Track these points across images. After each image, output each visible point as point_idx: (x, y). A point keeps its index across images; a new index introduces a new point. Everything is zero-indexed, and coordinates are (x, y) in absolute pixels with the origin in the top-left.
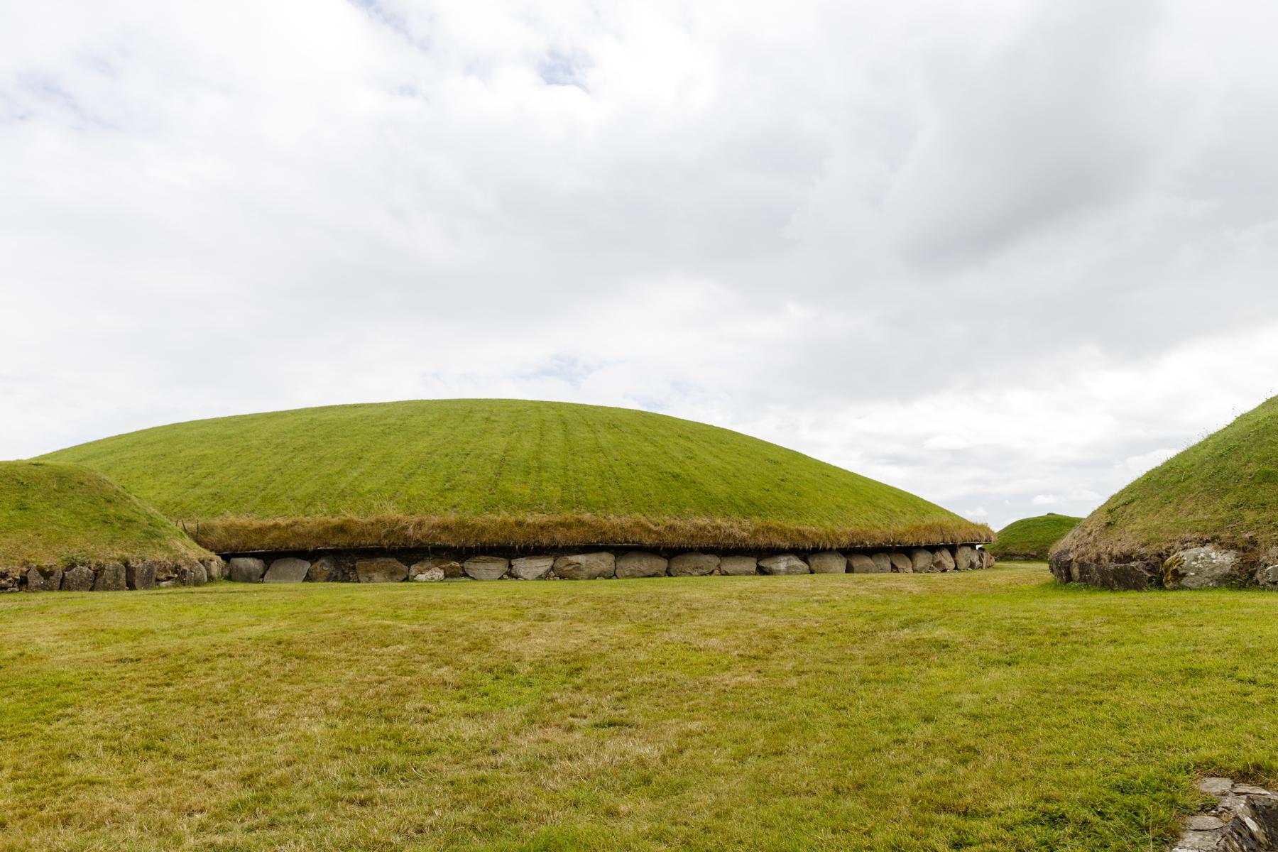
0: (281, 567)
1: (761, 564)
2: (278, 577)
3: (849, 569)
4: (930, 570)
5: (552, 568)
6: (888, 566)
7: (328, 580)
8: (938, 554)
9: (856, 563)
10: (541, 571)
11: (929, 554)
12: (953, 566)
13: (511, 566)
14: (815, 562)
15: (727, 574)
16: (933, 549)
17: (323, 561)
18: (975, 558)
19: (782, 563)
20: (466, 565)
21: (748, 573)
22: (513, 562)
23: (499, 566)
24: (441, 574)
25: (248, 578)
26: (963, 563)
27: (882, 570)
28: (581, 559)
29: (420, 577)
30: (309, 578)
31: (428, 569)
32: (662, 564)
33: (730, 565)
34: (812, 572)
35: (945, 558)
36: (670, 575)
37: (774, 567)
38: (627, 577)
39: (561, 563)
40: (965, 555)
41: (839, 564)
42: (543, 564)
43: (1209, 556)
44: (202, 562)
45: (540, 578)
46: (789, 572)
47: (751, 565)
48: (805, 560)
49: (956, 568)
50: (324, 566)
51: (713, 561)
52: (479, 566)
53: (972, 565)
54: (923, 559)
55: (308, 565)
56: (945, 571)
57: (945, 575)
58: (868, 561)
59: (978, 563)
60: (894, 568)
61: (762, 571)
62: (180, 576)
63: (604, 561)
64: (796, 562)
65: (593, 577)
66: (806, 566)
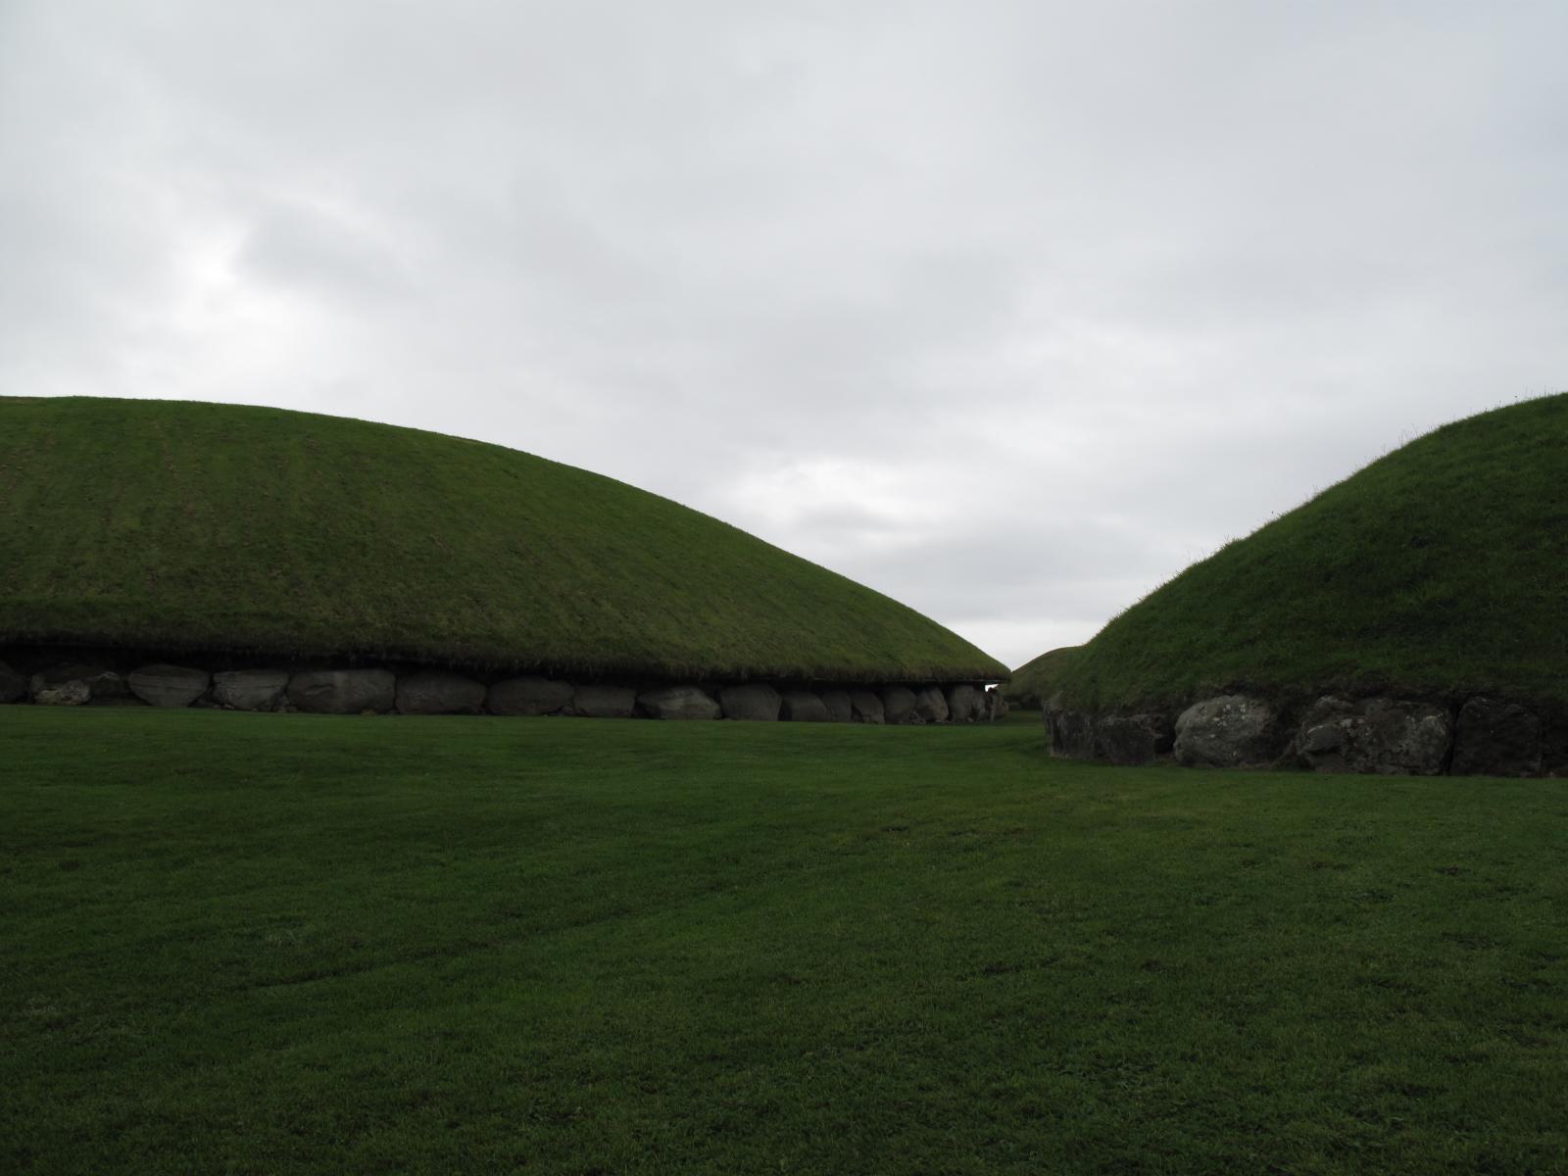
1: (642, 699)
3: (785, 715)
4: (910, 721)
5: (285, 690)
6: (848, 711)
8: (924, 695)
9: (799, 704)
10: (266, 694)
11: (912, 695)
12: (946, 714)
13: (212, 684)
14: (730, 698)
15: (583, 714)
16: (918, 687)
19: (677, 701)
20: (132, 678)
21: (618, 714)
22: (216, 678)
23: (193, 685)
24: (85, 693)
26: (962, 710)
28: (339, 678)
29: (47, 694)
31: (63, 681)
32: (475, 692)
33: (591, 700)
35: (936, 702)
36: (490, 713)
37: (663, 706)
38: (415, 711)
40: (963, 697)
41: (766, 703)
42: (264, 686)
43: (1237, 710)
45: (261, 707)
46: (687, 714)
47: (624, 700)
48: (716, 698)
49: (949, 718)
51: (560, 691)
53: (974, 713)
54: (901, 702)
56: (931, 721)
57: (931, 729)
58: (816, 703)
59: (983, 711)
60: (857, 716)
61: (643, 712)
64: (700, 699)
65: (356, 709)
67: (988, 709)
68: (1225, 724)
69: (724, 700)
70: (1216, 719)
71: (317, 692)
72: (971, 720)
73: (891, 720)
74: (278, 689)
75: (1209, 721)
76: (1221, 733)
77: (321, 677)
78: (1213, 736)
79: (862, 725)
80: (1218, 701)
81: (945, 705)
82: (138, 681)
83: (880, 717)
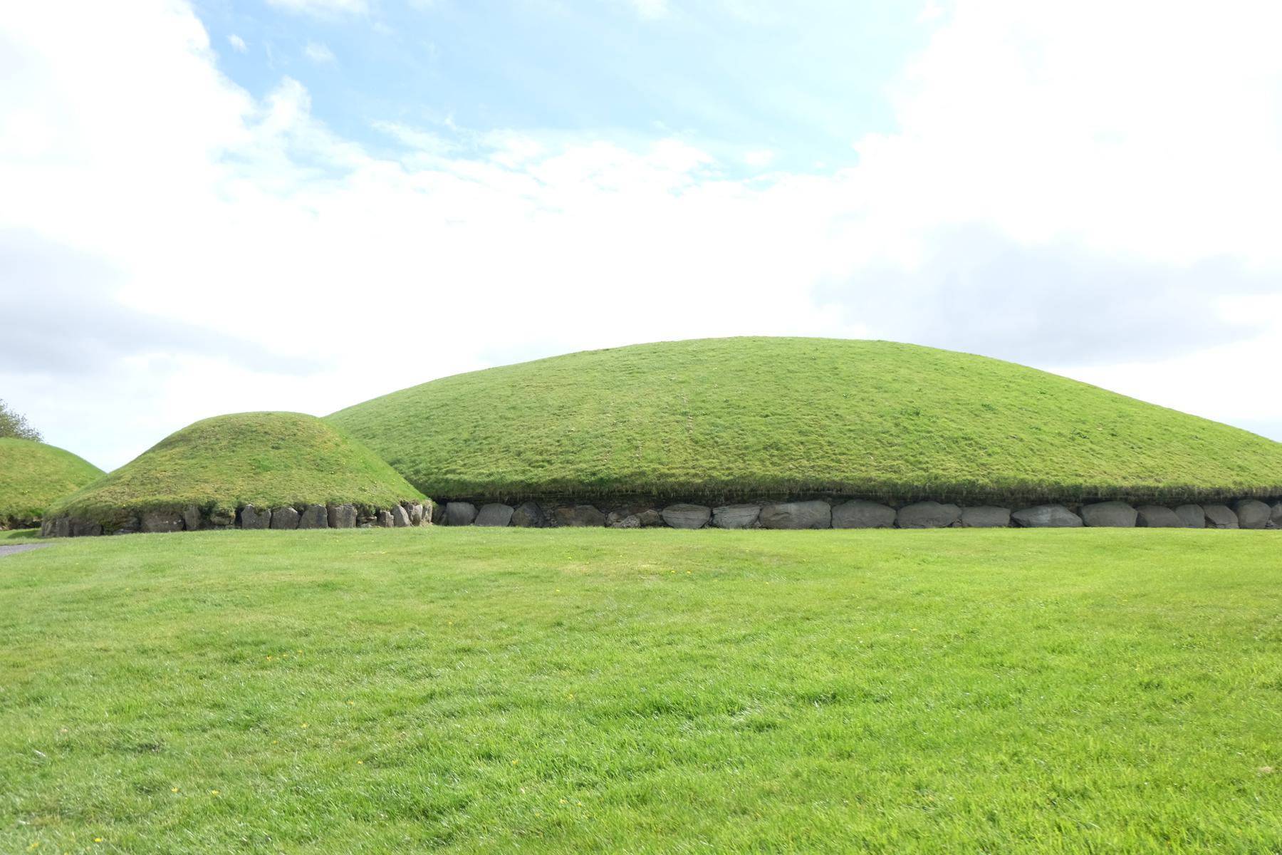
0: (489, 511)
1: (1016, 516)
2: (485, 523)
3: (1141, 523)
5: (758, 517)
7: (528, 526)
10: (746, 520)
11: (1265, 506)
13: (712, 515)
17: (524, 507)
19: (1045, 514)
22: (715, 511)
25: (460, 521)
28: (792, 508)
30: (512, 523)
32: (890, 514)
33: (973, 514)
37: (1033, 520)
39: (768, 512)
44: (404, 505)
46: (1053, 524)
50: (526, 512)
52: (678, 514)
55: (511, 510)
61: (1016, 524)
62: (368, 516)
63: (820, 509)
66: (1079, 520)
69: (1084, 512)
71: (778, 518)
74: (753, 517)
77: (781, 508)
82: (666, 513)
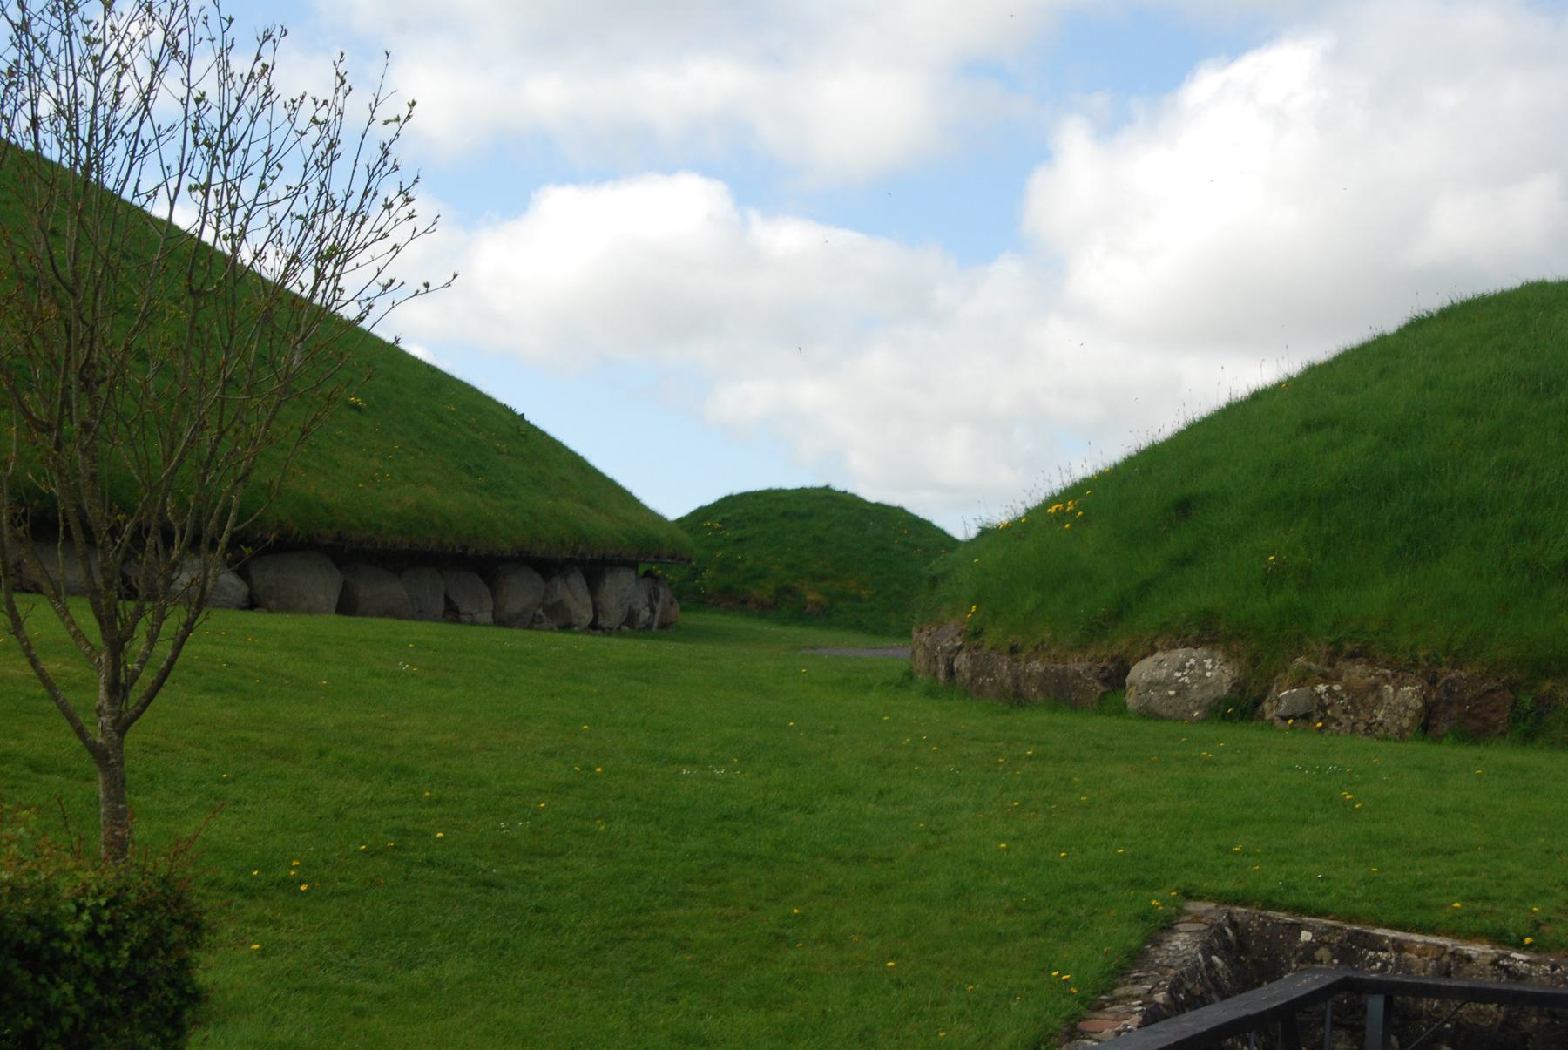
3: (347, 606)
4: (532, 624)
6: (440, 606)
12: (588, 617)
16: (547, 567)
18: (641, 603)
26: (614, 617)
27: (420, 615)
34: (252, 604)
40: (622, 590)
41: (322, 583)
43: (1202, 665)
53: (631, 619)
54: (522, 592)
56: (567, 627)
58: (394, 589)
59: (645, 614)
60: (452, 613)
66: (244, 589)
67: (653, 611)
68: (1187, 680)
70: (1178, 674)
72: (625, 628)
73: (501, 621)
75: (1170, 675)
76: (1182, 689)
78: (1172, 693)
79: (566, 638)
80: (1180, 653)
81: (589, 600)
83: (487, 616)
